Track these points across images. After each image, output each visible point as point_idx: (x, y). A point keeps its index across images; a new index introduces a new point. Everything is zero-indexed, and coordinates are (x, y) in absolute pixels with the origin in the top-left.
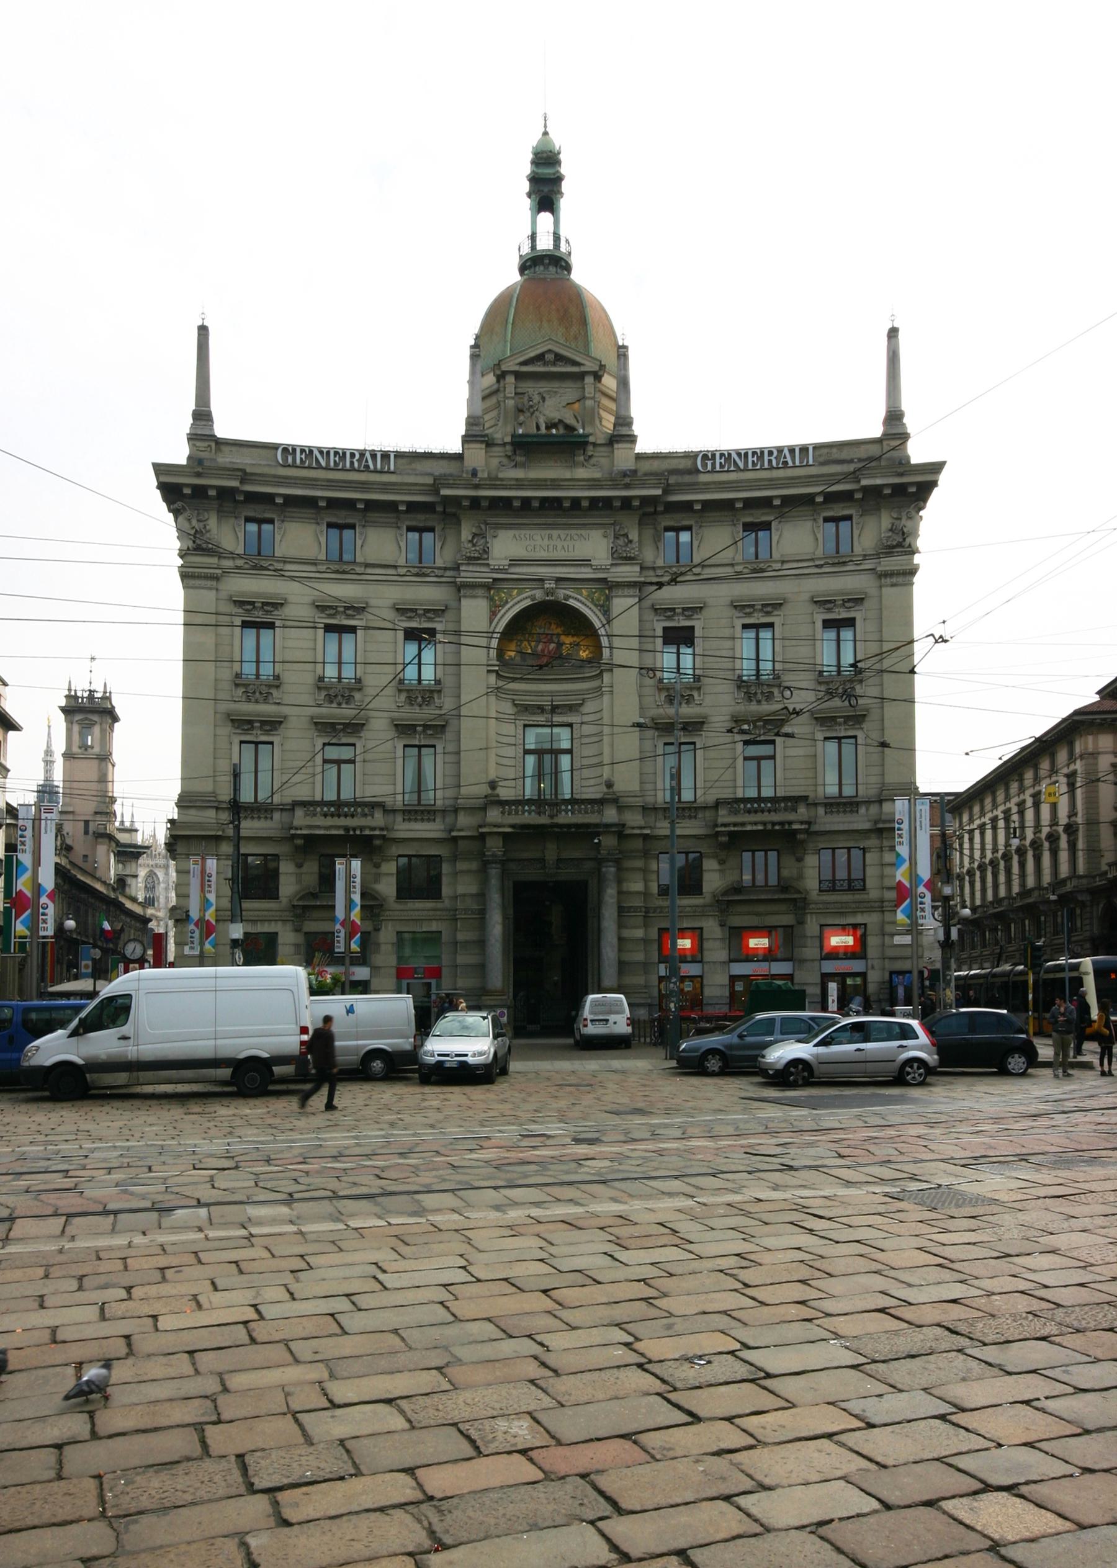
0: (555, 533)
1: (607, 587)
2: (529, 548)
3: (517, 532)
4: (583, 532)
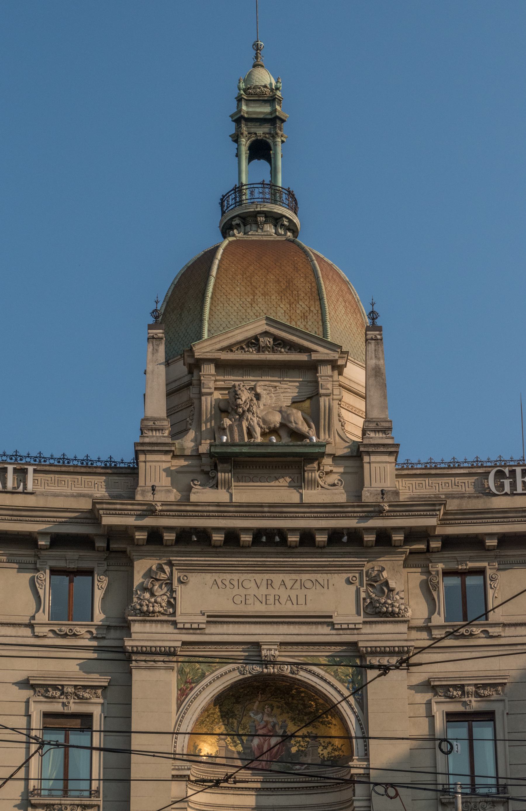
0: (277, 578)
1: (357, 661)
2: (238, 600)
3: (219, 577)
4: (320, 577)
